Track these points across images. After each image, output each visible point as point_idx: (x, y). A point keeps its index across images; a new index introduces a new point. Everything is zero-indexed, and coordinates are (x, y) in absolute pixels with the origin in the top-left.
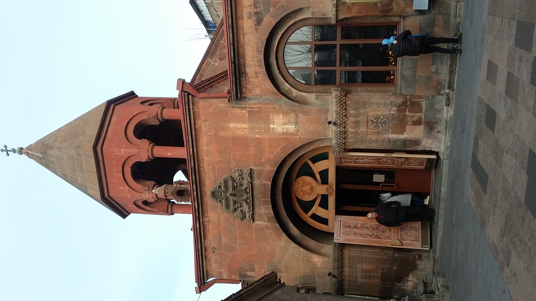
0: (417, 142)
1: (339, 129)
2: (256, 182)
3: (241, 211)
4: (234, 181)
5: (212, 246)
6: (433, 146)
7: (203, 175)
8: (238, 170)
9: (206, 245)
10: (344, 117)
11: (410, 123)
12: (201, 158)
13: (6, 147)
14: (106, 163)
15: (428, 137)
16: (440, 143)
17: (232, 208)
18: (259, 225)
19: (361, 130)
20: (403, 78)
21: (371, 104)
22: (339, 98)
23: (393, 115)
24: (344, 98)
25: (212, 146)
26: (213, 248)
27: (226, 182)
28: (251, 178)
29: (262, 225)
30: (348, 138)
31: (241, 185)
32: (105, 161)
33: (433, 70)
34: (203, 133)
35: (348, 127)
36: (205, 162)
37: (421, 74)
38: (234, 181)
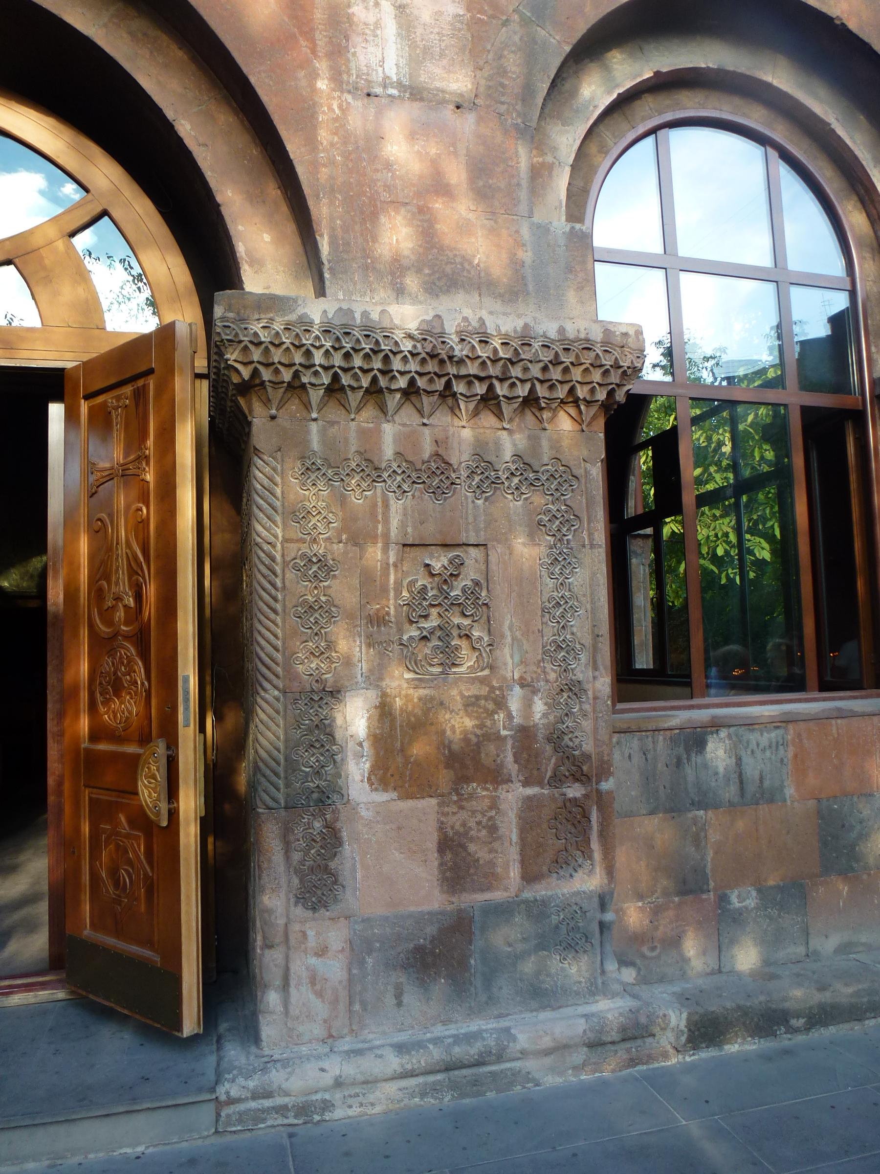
0: (319, 886)
1: (407, 346)
6: (301, 995)
10: (480, 389)
11: (455, 821)
15: (358, 950)
16: (329, 1043)
19: (396, 506)
20: (695, 740)
21: (561, 560)
22: (608, 362)
23: (501, 704)
24: (601, 395)
30: (333, 412)
33: (735, 902)
35: (408, 416)
37: (714, 836)
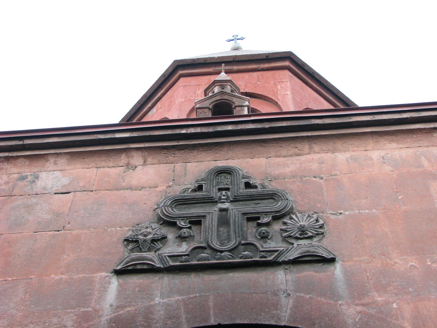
2: (281, 277)
3: (164, 238)
4: (278, 217)
5: (43, 175)
7: (284, 151)
8: (321, 227)
9: (52, 160)
12: (339, 144)
13: (242, 39)
14: (255, 74)
17: (177, 212)
18: (104, 290)
25: (388, 168)
26: (37, 177)
27: (272, 196)
28: (296, 262)
29: (101, 298)
31: (264, 237)
32: (259, 73)
34: (420, 150)
36: (329, 155)
38: (278, 217)
